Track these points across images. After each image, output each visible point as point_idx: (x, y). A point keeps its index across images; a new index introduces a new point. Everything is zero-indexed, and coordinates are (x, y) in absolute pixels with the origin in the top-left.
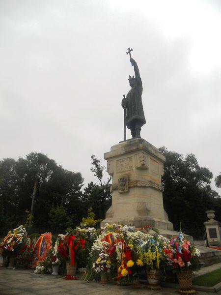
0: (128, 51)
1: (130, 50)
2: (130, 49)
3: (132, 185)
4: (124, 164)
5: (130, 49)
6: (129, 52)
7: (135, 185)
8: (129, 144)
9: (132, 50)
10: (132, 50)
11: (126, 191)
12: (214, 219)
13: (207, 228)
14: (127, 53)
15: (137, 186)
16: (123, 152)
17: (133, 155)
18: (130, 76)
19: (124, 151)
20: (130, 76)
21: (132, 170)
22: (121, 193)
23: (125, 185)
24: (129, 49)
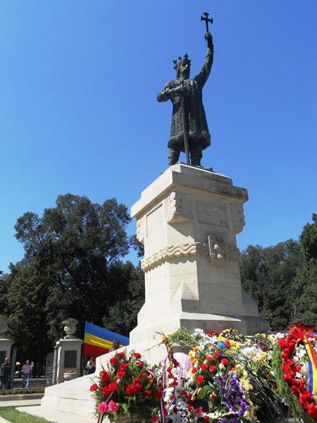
0: (204, 17)
5: (204, 17)
9: (211, 21)
14: (202, 18)
20: (186, 56)
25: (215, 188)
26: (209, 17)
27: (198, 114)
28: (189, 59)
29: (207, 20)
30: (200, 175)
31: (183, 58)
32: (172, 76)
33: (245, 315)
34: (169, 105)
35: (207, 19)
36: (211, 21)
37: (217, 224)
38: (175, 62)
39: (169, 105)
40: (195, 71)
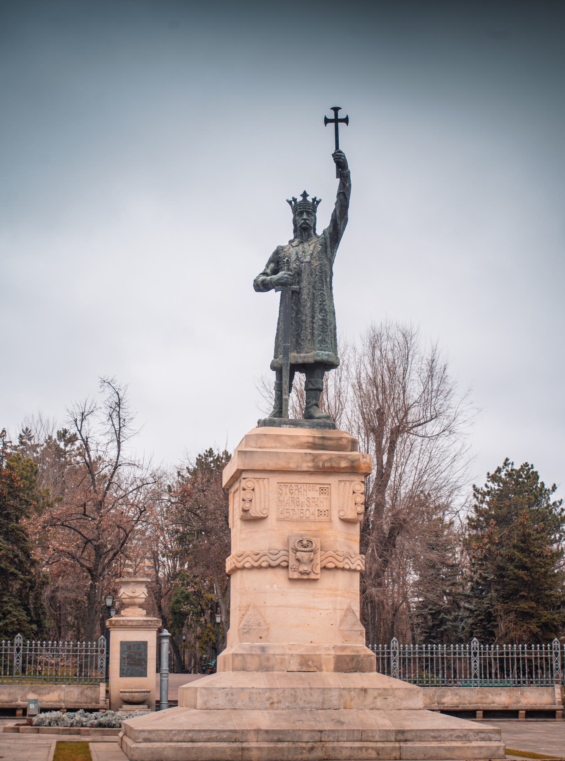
0: (331, 116)
1: (336, 120)
2: (341, 115)
3: (331, 565)
4: (302, 499)
6: (336, 121)
7: (340, 565)
8: (317, 441)
10: (346, 120)
11: (312, 576)
12: (141, 606)
13: (118, 637)
14: (327, 121)
15: (343, 569)
16: (306, 466)
17: (333, 480)
18: (305, 195)
19: (311, 464)
20: (305, 195)
21: (330, 521)
22: (291, 580)
23: (312, 561)
24: (336, 110)
25: (311, 464)
26: (341, 115)
27: (313, 317)
28: (309, 199)
29: (336, 121)
30: (290, 442)
31: (300, 199)
32: (283, 233)
33: (339, 644)
34: (274, 297)
35: (336, 120)
36: (346, 120)
37: (312, 518)
38: (290, 202)
39: (274, 297)
40: (323, 222)
